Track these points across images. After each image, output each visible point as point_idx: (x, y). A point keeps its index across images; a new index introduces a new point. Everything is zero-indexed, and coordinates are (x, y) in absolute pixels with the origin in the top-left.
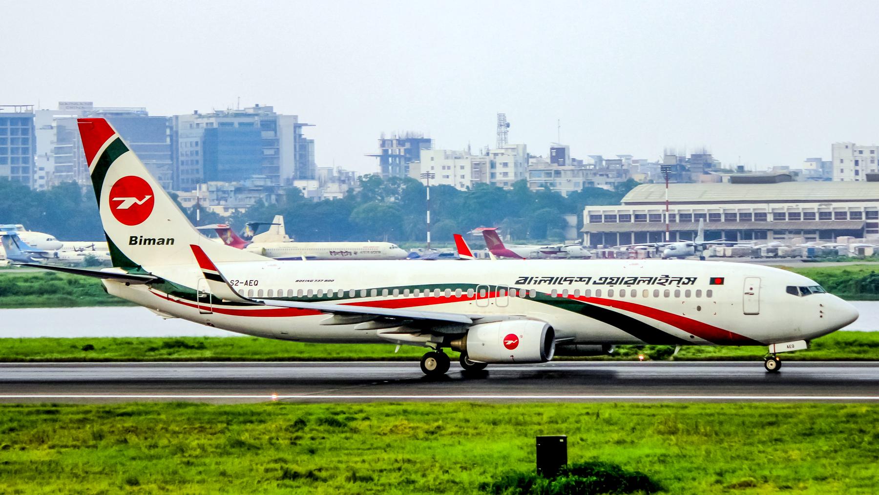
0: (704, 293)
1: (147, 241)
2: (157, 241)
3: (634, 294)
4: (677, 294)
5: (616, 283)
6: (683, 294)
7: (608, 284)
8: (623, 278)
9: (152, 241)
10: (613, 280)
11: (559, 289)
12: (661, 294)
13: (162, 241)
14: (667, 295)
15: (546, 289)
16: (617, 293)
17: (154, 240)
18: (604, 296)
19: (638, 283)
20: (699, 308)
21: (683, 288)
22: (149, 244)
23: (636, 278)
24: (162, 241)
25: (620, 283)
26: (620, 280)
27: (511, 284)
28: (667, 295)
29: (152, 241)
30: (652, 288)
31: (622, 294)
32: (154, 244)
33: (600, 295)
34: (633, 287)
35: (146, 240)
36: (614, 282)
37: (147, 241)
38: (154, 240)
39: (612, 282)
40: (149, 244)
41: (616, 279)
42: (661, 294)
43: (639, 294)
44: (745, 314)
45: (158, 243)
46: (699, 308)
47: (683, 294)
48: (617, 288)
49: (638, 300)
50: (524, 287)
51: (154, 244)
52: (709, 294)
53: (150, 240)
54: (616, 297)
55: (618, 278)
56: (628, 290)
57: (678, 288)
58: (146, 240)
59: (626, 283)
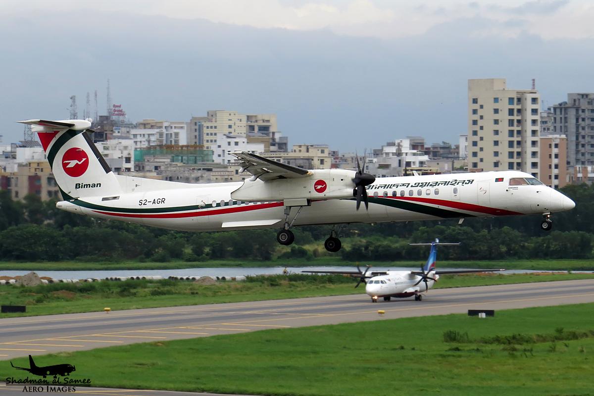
5: (425, 186)
8: (429, 183)
32: (89, 187)
35: (85, 185)
38: (89, 185)
55: (426, 183)
58: (85, 185)
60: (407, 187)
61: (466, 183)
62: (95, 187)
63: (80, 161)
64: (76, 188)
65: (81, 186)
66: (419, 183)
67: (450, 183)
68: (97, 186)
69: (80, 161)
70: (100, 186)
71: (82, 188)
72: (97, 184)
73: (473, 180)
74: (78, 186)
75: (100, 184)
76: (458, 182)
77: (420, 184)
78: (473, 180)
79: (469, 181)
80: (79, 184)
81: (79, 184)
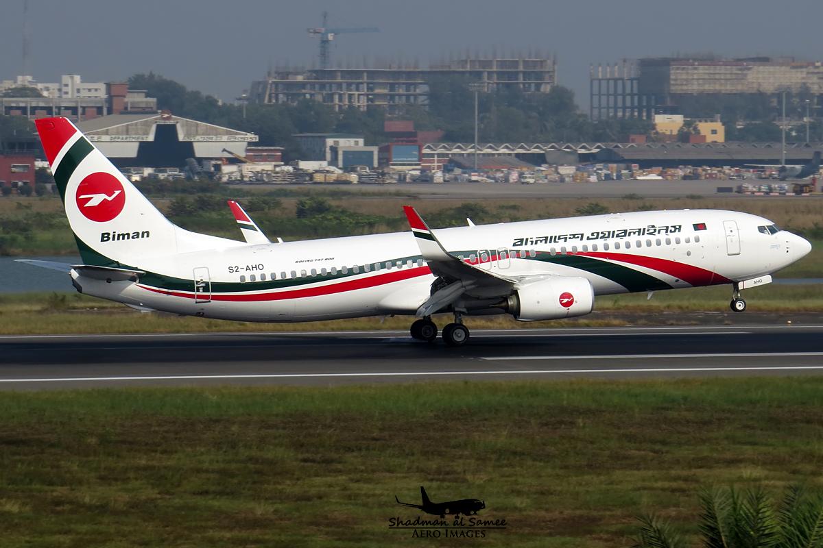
0: (692, 240)
1: (121, 237)
2: (131, 235)
3: (628, 246)
4: (668, 242)
5: (608, 237)
6: (673, 241)
7: (601, 238)
8: (614, 232)
9: (126, 236)
11: (558, 247)
12: (654, 243)
13: (136, 235)
14: (659, 243)
16: (612, 245)
17: (128, 234)
18: (601, 250)
19: (629, 235)
20: (689, 254)
21: (672, 236)
22: (123, 239)
23: (626, 231)
24: (136, 235)
25: (613, 237)
26: (610, 234)
27: (510, 247)
28: (659, 243)
29: (126, 236)
30: (644, 239)
31: (617, 247)
32: (128, 238)
33: (597, 250)
34: (627, 239)
35: (119, 235)
36: (607, 236)
37: (121, 237)
38: (128, 234)
39: (604, 236)
40: (123, 239)
41: (607, 233)
42: (654, 243)
44: (729, 255)
45: (133, 238)
46: (689, 254)
47: (673, 241)
49: (633, 251)
50: (523, 248)
51: (128, 238)
52: (697, 240)
53: (123, 235)
54: (612, 250)
56: (622, 242)
58: (119, 235)
59: (618, 236)
60: (581, 239)
61: (671, 231)
62: (138, 237)
63: (110, 196)
64: (102, 240)
65: (111, 236)
66: (598, 233)
67: (646, 232)
68: (143, 237)
69: (110, 196)
70: (148, 236)
71: (114, 239)
72: (143, 233)
73: (680, 226)
74: (105, 237)
75: (148, 233)
76: (657, 229)
77: (601, 235)
78: (680, 226)
79: (674, 227)
80: (109, 234)
81: (109, 234)
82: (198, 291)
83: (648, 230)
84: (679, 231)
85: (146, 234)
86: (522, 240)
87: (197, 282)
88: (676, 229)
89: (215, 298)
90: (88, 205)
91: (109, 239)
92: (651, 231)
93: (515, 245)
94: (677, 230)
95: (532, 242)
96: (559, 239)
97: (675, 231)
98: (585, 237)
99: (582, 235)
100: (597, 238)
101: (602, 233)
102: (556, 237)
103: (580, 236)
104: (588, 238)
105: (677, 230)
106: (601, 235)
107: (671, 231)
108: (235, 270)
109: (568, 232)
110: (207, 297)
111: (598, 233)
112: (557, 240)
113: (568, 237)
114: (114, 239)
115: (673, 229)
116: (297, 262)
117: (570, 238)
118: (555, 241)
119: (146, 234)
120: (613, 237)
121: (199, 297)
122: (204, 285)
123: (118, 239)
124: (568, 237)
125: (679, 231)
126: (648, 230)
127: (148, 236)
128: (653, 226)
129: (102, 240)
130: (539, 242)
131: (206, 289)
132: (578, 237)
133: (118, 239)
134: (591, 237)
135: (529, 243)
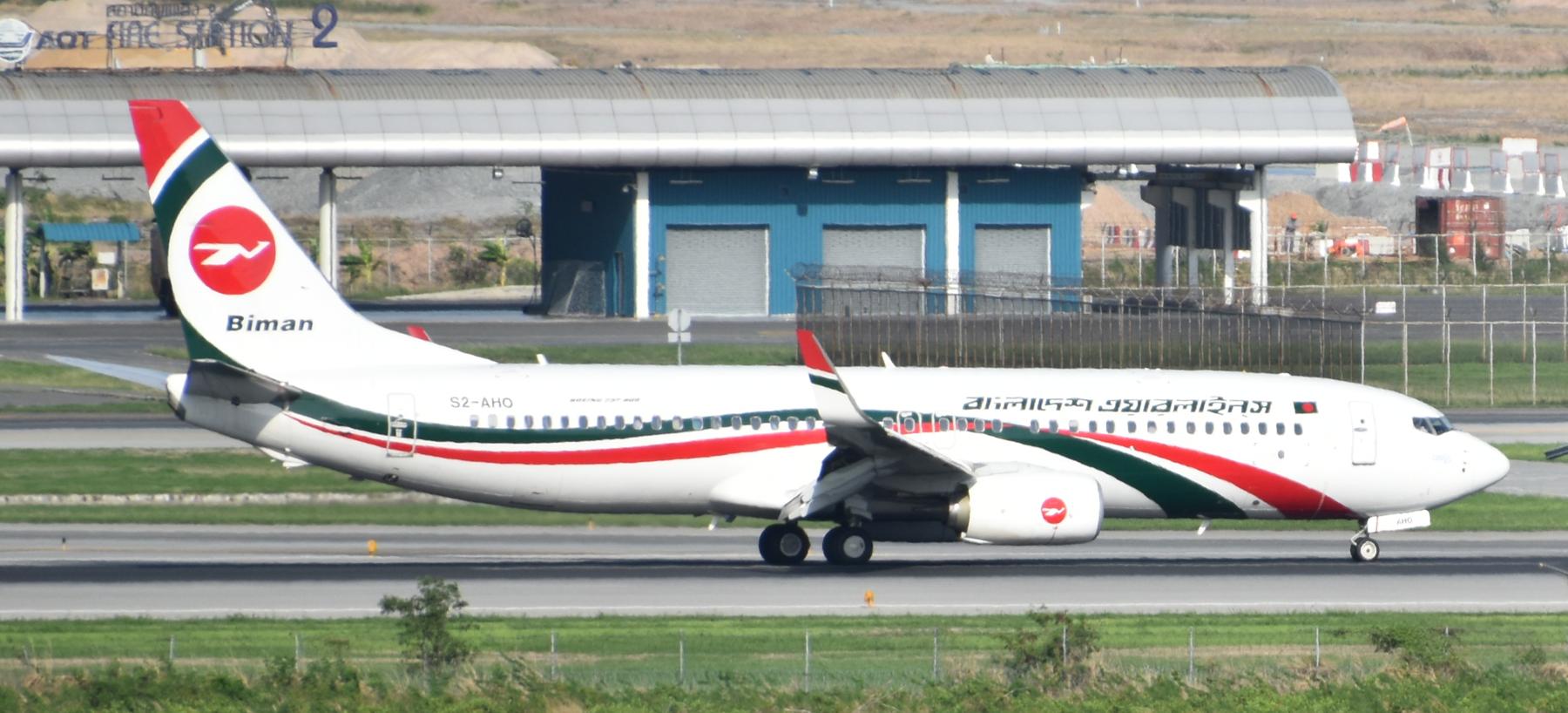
0: (1289, 429)
1: (263, 325)
2: (280, 325)
5: (1137, 410)
9: (271, 325)
10: (1131, 405)
15: (1022, 418)
17: (276, 323)
21: (1253, 420)
22: (267, 328)
25: (1145, 410)
29: (271, 325)
30: (1200, 419)
32: (275, 328)
35: (259, 323)
36: (1134, 408)
37: (263, 325)
40: (267, 328)
43: (1181, 428)
44: (1354, 464)
45: (284, 328)
48: (1141, 419)
51: (275, 328)
52: (1298, 430)
53: (267, 323)
54: (1142, 434)
56: (1162, 420)
57: (1244, 420)
59: (1154, 409)
60: (1088, 408)
61: (1252, 411)
64: (230, 328)
65: (245, 323)
67: (1207, 407)
69: (250, 248)
70: (310, 328)
71: (249, 328)
73: (1269, 404)
74: (234, 323)
75: (310, 323)
77: (1123, 406)
79: (1259, 404)
80: (241, 318)
81: (241, 318)
82: (394, 434)
83: (1211, 405)
84: (1267, 411)
85: (306, 325)
86: (980, 401)
87: (393, 419)
88: (1261, 407)
89: (421, 450)
90: (209, 262)
91: (240, 326)
92: (1217, 406)
93: (966, 407)
94: (1264, 410)
95: (998, 406)
96: (1048, 403)
97: (1259, 411)
98: (1094, 407)
99: (1090, 403)
100: (1116, 410)
101: (1126, 402)
102: (1041, 401)
103: (1086, 404)
104: (1100, 409)
105: (1264, 410)
106: (1123, 406)
107: (1252, 411)
108: (462, 403)
109: (1065, 396)
110: (407, 448)
111: (1118, 404)
112: (1043, 406)
113: (1064, 402)
114: (249, 328)
115: (1256, 407)
116: (573, 400)
117: (1067, 405)
118: (1040, 408)
119: (306, 325)
120: (1145, 410)
121: (395, 446)
122: (404, 425)
123: (258, 328)
124: (1064, 402)
125: (1267, 411)
126: (1211, 405)
127: (310, 328)
128: (1220, 399)
129: (230, 328)
130: (1010, 406)
131: (407, 433)
132: (1081, 405)
133: (258, 328)
134: (1105, 407)
135: (993, 405)
